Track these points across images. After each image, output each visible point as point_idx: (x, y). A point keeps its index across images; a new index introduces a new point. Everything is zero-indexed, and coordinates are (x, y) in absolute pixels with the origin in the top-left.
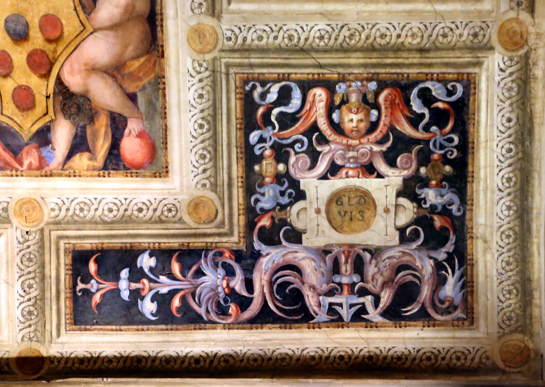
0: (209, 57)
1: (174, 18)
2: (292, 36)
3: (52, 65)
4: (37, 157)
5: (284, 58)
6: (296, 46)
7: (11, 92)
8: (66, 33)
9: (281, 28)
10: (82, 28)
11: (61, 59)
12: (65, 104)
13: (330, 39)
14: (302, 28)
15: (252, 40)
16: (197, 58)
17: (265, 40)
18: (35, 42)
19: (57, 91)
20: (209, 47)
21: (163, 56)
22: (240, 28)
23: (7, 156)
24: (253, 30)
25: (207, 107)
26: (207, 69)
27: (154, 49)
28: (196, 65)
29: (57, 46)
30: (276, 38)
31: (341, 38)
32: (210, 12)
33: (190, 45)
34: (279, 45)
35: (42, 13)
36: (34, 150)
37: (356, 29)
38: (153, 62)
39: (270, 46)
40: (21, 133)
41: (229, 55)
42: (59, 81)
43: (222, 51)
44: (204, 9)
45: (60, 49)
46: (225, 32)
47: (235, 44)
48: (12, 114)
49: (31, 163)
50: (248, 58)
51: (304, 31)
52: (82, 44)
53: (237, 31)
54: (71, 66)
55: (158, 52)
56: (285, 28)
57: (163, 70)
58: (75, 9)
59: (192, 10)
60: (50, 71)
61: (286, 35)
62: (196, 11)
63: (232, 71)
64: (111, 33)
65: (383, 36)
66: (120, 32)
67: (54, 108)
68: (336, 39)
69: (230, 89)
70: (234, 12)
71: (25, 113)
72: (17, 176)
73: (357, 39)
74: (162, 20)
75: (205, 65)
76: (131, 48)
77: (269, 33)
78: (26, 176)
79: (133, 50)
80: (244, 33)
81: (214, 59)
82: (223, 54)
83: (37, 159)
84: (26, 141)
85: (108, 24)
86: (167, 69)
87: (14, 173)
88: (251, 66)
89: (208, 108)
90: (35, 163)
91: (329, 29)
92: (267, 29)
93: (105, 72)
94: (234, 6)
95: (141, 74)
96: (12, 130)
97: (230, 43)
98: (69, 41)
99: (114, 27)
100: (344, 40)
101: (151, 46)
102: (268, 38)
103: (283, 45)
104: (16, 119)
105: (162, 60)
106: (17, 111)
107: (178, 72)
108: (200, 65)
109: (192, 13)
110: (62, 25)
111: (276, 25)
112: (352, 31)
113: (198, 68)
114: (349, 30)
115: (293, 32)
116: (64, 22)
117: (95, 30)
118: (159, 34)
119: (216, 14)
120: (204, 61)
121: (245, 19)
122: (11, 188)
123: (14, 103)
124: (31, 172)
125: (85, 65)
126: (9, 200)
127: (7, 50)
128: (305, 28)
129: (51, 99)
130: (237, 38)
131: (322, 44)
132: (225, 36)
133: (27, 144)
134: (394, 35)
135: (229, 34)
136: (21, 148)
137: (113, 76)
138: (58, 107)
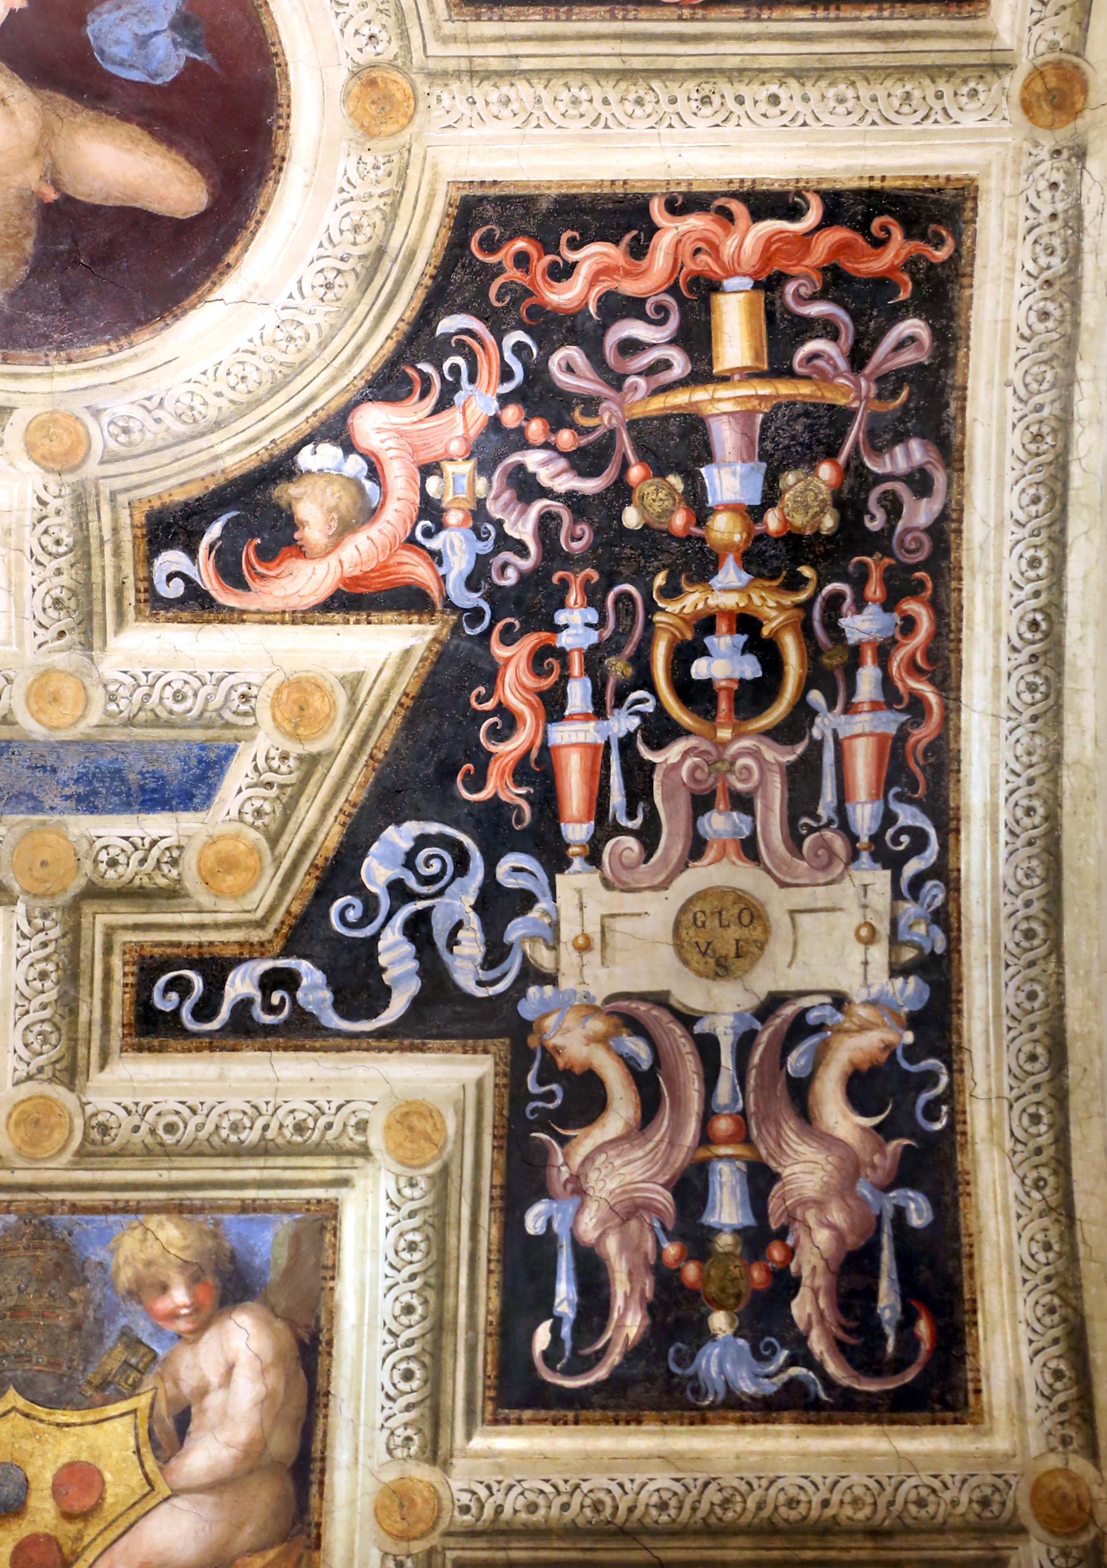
1: (349, 1468)
13: (680, 1508)
15: (515, 1511)
16: (394, 1550)
17: (542, 1511)
20: (422, 1527)
22: (489, 1487)
24: (517, 1490)
30: (565, 1507)
31: (704, 1507)
32: (428, 1454)
33: (379, 1523)
34: (573, 1521)
37: (735, 1489)
39: (553, 1524)
41: (462, 1542)
43: (448, 1534)
44: (414, 1449)
46: (457, 1495)
47: (478, 1520)
50: (504, 1549)
53: (483, 1493)
59: (390, 1451)
62: (399, 1453)
65: (792, 1503)
68: (694, 1509)
70: (477, 1455)
73: (739, 1508)
77: (551, 1497)
80: (498, 1498)
81: (431, 1552)
82: (451, 1542)
91: (678, 1488)
92: (548, 1488)
94: (478, 1443)
97: (467, 1518)
100: (711, 1511)
102: (549, 1507)
103: (580, 1521)
109: (388, 1458)
111: (566, 1481)
112: (727, 1493)
114: (720, 1490)
119: (440, 1460)
120: (409, 1556)
121: (501, 1468)
131: (664, 1518)
132: (457, 1503)
134: (816, 1500)
135: (465, 1498)
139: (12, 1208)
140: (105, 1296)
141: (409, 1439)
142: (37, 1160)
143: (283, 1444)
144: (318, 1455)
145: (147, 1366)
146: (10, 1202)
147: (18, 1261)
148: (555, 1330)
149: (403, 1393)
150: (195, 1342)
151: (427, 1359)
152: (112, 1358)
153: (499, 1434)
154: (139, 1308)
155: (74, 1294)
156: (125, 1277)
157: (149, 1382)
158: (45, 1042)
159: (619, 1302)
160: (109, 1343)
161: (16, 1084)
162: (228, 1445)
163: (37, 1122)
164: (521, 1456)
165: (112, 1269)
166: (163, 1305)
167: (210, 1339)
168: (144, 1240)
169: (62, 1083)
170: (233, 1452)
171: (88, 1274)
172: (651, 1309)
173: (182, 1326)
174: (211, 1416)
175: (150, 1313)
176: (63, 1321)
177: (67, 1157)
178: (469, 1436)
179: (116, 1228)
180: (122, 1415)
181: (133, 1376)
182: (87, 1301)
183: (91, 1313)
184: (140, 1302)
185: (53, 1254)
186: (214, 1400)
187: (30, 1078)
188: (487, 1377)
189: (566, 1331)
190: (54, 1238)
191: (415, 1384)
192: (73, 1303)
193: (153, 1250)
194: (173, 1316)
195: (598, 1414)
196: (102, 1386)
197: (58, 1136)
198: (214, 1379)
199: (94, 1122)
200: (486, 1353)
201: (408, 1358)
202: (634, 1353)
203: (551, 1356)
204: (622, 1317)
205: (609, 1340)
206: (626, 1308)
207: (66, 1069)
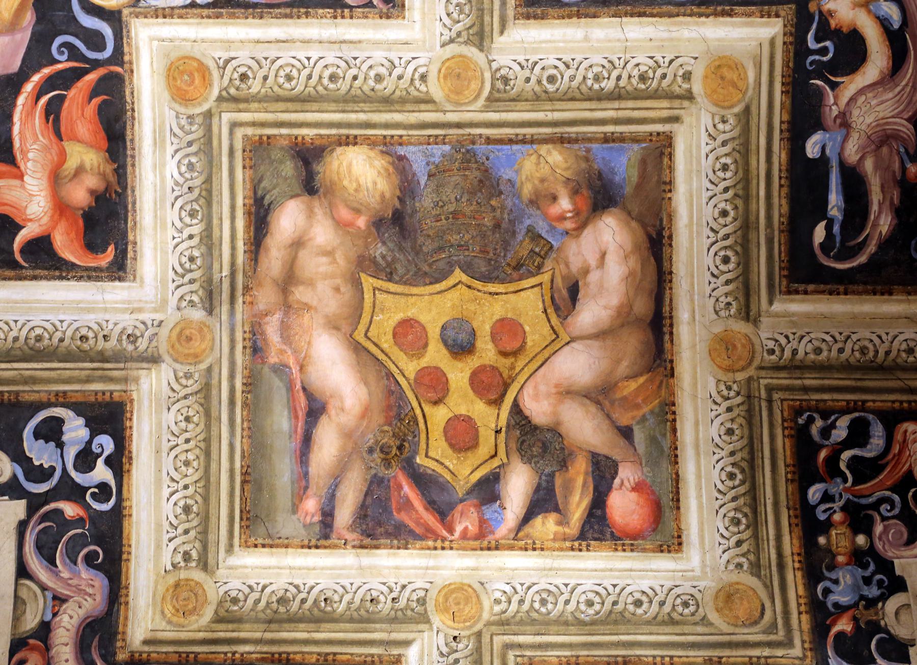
0: (740, 376)
1: (689, 323)
2: (867, 348)
3: (506, 386)
4: (477, 519)
5: (855, 379)
6: (872, 362)
7: (443, 424)
8: (529, 343)
9: (849, 337)
10: (554, 336)
11: (521, 379)
12: (523, 442)
14: (880, 337)
15: (806, 353)
17: (825, 354)
18: (484, 355)
19: (513, 422)
20: (742, 363)
21: (672, 375)
22: (787, 337)
23: (430, 519)
25: (739, 447)
26: (738, 394)
27: (659, 366)
28: (723, 387)
29: (516, 361)
30: (841, 350)
32: (743, 314)
33: (713, 360)
34: (847, 360)
35: (496, 317)
36: (472, 509)
38: (657, 383)
39: (834, 362)
40: (454, 484)
41: (770, 373)
42: (517, 409)
43: (761, 368)
44: (733, 311)
45: (520, 364)
46: (765, 342)
47: (780, 359)
48: (442, 456)
49: (466, 528)
50: (800, 378)
51: (883, 342)
52: (552, 358)
53: (783, 341)
54: (535, 387)
55: (666, 369)
56: (854, 337)
57: (673, 394)
58: (545, 311)
59: (716, 312)
60: (503, 396)
61: (856, 347)
62: (722, 313)
63: (776, 396)
64: (595, 344)
66: (609, 342)
67: (506, 447)
69: (775, 423)
70: (777, 315)
71: (463, 454)
72: (443, 548)
74: (671, 325)
75: (735, 387)
76: (625, 364)
77: (831, 344)
78: (457, 549)
79: (627, 366)
80: (794, 344)
81: (749, 380)
82: (763, 373)
83: (477, 523)
84: (460, 495)
85: (593, 331)
86: (678, 393)
87: (439, 544)
88: (806, 389)
89: (741, 449)
90: (473, 529)
92: (828, 338)
93: (585, 396)
94: (777, 307)
95: (639, 400)
96: (441, 480)
97: (773, 357)
98: (534, 354)
99: (601, 335)
101: (655, 361)
102: (830, 351)
103: (852, 360)
104: (447, 463)
105: (671, 381)
106: (450, 451)
107: (695, 396)
108: (729, 388)
109: (715, 317)
110: (525, 333)
111: (841, 334)
113: (725, 393)
115: (867, 343)
116: (527, 328)
117: (573, 340)
118: (667, 345)
119: (752, 318)
120: (734, 382)
121: (794, 324)
122: (433, 568)
123: (446, 440)
124: (465, 543)
125: (557, 386)
126: (427, 586)
127: (442, 366)
128: (884, 337)
129: (503, 434)
130: (783, 350)
132: (765, 348)
133: (462, 501)
135: (771, 344)
136: (452, 506)
137: (598, 403)
138: (513, 445)
139: (447, 140)
140: (514, 204)
141: (729, 304)
142: (462, 104)
143: (643, 307)
144: (667, 314)
145: (546, 253)
146: (445, 136)
147: (454, 179)
148: (829, 228)
149: (723, 273)
150: (578, 236)
151: (739, 249)
152: (523, 247)
153: (792, 301)
154: (538, 212)
155: (493, 202)
156: (527, 190)
157: (549, 264)
158: (461, 12)
159: (875, 207)
160: (520, 237)
161: (443, 45)
162: (605, 308)
163: (459, 76)
164: (808, 316)
165: (518, 185)
166: (555, 210)
167: (588, 233)
168: (538, 164)
169: (475, 45)
170: (609, 312)
171: (502, 188)
172: (899, 212)
173: (569, 225)
174: (593, 288)
175: (546, 216)
176: (488, 221)
177: (481, 102)
178: (771, 303)
179: (519, 155)
180: (532, 287)
181: (538, 259)
182: (503, 208)
183: (506, 216)
184: (538, 208)
185: (477, 174)
186: (593, 277)
187: (452, 41)
188: (781, 261)
189: (836, 229)
190: (476, 162)
191: (731, 266)
192: (494, 209)
193: (545, 170)
194: (562, 218)
195: (861, 288)
196: (518, 267)
197: (474, 86)
198: (593, 263)
199: (498, 75)
200: (780, 245)
201: (726, 248)
202: (885, 244)
203: (826, 247)
204: (877, 218)
205: (868, 235)
206: (880, 213)
207: (476, 34)
